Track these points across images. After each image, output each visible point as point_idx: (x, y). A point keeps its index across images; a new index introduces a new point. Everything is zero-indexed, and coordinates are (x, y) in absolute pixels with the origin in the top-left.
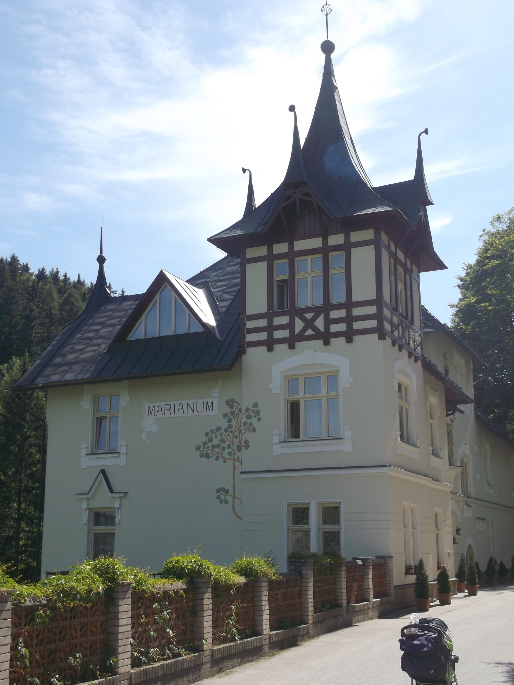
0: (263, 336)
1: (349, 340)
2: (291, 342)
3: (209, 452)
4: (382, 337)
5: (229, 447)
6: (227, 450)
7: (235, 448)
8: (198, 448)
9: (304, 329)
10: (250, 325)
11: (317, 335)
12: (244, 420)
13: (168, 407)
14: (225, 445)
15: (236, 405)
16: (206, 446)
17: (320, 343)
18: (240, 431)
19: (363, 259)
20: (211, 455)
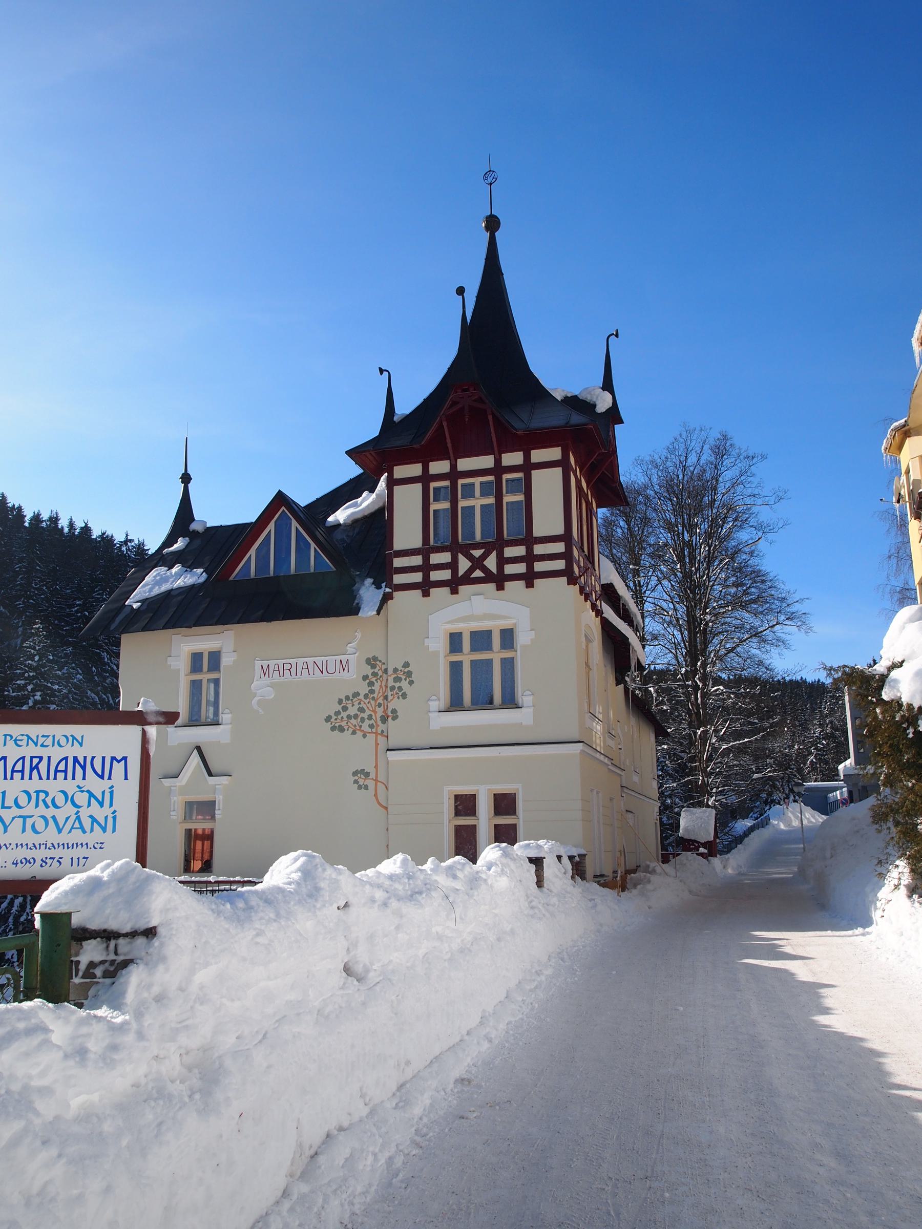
0: (417, 577)
1: (530, 585)
2: (453, 585)
3: (344, 724)
4: (572, 581)
5: (370, 718)
6: (367, 722)
7: (379, 719)
8: (328, 719)
9: (471, 570)
10: (398, 562)
11: (489, 577)
12: (391, 683)
13: (287, 667)
14: (365, 715)
15: (380, 664)
16: (339, 717)
17: (492, 586)
18: (386, 698)
19: (548, 487)
20: (346, 728)
